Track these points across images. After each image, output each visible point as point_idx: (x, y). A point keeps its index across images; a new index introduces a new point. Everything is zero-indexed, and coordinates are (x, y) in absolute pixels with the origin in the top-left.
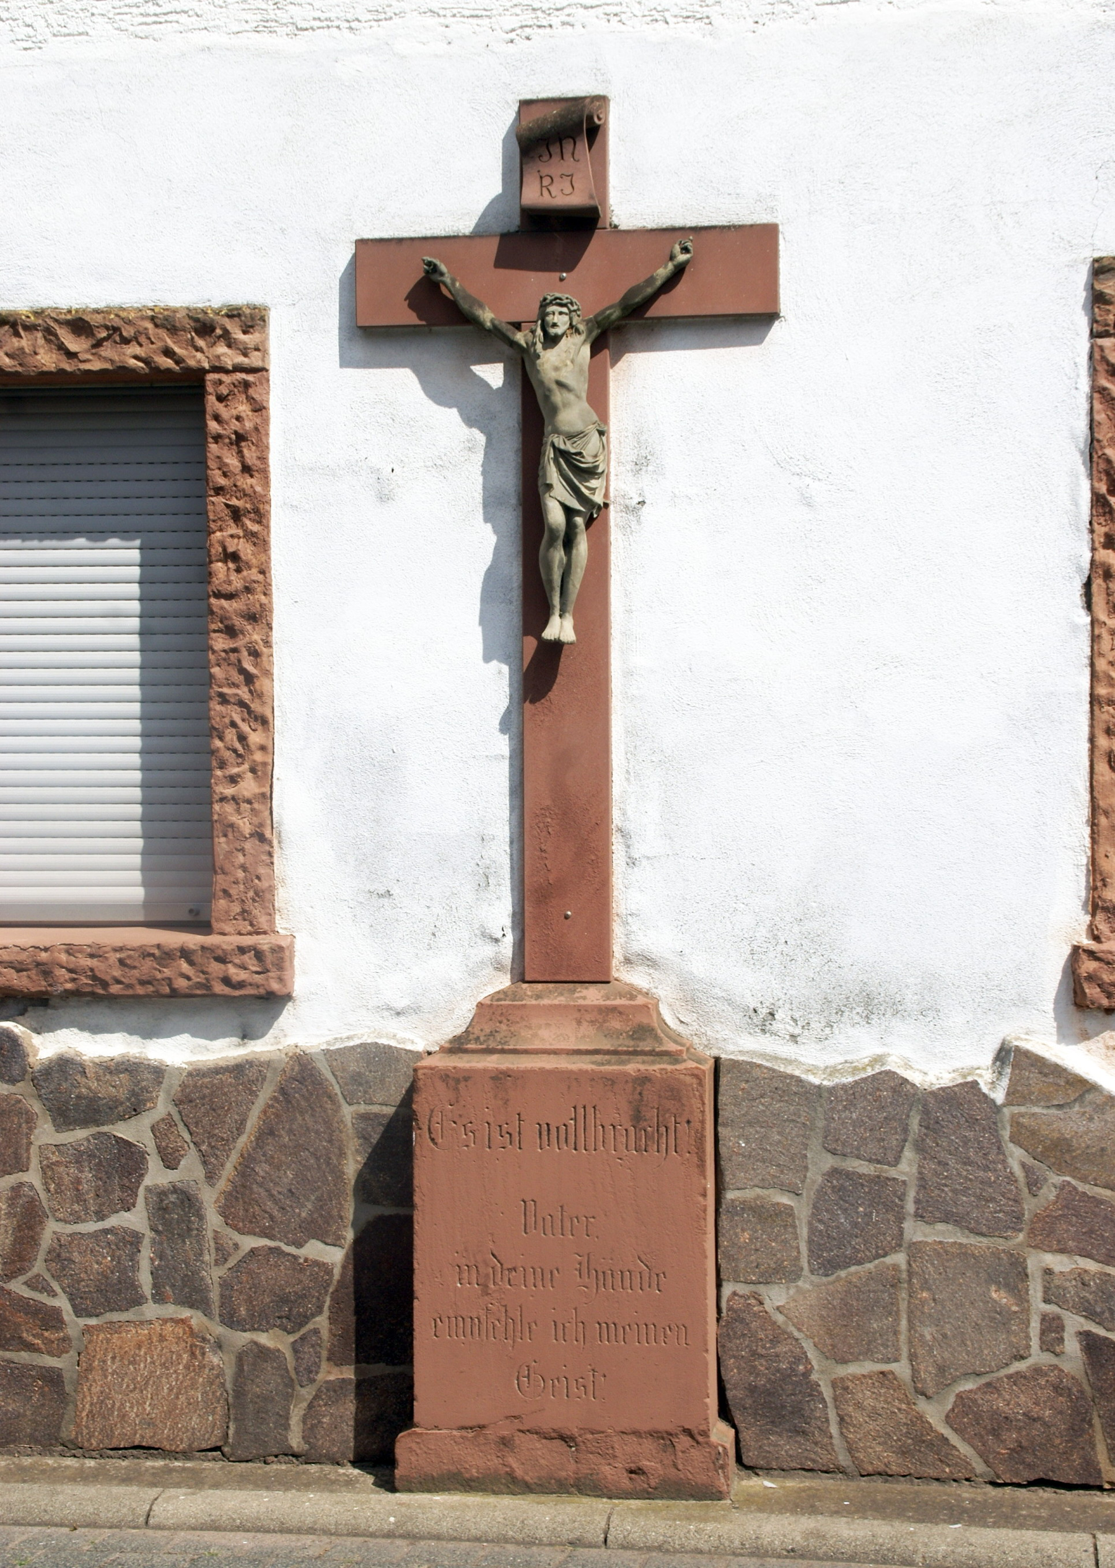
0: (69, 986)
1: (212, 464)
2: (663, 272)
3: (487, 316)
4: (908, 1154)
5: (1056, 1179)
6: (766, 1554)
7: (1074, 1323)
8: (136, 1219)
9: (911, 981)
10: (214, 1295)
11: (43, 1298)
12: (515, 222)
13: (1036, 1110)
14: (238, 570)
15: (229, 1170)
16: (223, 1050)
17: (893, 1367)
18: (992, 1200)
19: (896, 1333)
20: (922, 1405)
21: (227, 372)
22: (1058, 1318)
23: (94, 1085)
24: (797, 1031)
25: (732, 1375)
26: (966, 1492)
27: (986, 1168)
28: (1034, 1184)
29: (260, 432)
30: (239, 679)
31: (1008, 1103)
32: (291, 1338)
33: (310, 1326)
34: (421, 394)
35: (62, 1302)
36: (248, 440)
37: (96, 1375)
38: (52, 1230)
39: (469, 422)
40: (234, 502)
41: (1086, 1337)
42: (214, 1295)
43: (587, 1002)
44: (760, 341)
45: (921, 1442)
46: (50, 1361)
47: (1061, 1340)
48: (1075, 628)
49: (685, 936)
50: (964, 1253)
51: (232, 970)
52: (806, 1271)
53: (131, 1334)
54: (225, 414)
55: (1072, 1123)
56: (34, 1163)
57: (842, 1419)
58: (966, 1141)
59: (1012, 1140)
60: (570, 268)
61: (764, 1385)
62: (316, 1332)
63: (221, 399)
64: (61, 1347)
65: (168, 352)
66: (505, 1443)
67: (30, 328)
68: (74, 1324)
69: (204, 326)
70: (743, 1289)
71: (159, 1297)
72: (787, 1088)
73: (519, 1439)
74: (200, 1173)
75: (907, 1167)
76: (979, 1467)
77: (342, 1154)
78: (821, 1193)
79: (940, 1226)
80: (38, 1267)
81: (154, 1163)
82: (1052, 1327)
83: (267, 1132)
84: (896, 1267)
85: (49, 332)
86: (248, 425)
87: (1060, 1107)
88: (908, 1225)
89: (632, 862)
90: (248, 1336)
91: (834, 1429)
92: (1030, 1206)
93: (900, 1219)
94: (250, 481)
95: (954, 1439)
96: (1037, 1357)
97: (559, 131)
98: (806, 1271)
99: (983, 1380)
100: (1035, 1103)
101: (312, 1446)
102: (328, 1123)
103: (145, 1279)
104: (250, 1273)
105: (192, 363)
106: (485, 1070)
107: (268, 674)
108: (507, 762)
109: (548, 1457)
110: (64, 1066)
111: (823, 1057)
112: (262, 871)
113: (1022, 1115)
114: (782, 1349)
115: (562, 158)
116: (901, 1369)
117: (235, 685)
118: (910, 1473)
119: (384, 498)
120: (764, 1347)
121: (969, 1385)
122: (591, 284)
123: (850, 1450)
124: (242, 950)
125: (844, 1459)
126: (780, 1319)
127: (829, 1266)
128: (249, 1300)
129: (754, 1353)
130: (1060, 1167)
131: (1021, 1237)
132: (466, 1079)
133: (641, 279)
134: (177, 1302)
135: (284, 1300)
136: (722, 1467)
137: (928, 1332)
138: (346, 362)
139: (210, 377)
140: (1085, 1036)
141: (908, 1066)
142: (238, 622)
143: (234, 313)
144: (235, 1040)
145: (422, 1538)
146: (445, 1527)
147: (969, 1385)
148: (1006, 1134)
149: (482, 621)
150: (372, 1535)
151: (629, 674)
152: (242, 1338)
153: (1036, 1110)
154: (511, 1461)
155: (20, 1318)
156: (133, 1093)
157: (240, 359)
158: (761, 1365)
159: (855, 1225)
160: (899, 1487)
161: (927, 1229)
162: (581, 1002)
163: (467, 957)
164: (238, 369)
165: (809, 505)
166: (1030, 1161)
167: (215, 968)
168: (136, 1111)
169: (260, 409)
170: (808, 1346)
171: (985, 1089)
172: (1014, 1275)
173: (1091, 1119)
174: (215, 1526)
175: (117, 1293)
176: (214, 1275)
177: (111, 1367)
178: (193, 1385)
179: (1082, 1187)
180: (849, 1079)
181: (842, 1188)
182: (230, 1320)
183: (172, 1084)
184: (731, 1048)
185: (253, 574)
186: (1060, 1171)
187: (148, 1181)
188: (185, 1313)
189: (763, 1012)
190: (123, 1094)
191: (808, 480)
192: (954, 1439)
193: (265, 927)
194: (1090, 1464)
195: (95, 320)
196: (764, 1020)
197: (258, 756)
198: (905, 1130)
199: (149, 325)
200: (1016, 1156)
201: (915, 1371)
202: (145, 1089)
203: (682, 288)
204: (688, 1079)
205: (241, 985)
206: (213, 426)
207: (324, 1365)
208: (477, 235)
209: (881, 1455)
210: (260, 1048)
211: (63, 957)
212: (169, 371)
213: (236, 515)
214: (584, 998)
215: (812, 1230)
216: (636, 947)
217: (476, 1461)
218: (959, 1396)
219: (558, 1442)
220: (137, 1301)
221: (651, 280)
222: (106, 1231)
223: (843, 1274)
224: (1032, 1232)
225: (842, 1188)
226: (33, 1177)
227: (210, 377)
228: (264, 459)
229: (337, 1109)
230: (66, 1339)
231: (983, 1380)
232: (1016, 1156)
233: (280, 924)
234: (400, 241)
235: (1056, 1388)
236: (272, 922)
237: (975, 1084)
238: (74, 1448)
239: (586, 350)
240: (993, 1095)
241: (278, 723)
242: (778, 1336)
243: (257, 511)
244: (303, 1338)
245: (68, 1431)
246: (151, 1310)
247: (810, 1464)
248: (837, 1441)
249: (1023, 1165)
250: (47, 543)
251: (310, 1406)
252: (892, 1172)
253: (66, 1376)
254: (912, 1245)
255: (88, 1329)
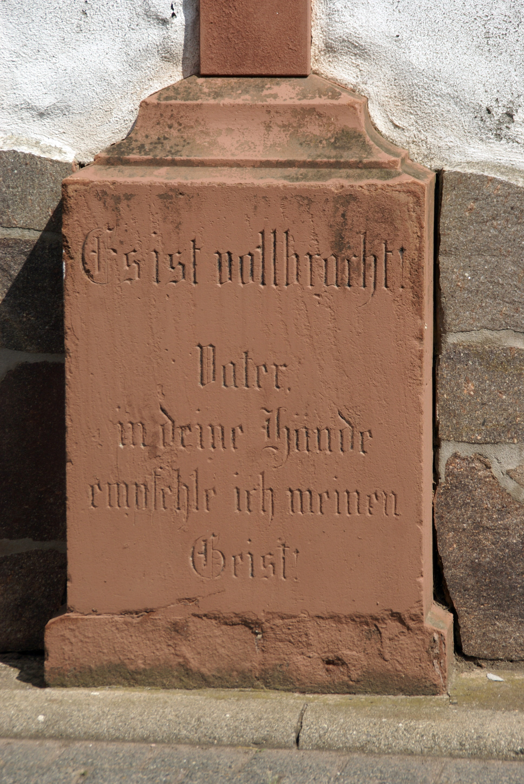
6: (490, 756)
25: (451, 552)
43: (279, 102)
61: (490, 563)
66: (177, 629)
70: (465, 450)
106: (151, 186)
114: (511, 520)
120: (490, 518)
126: (510, 485)
129: (478, 526)
132: (128, 197)
136: (438, 657)
145: (78, 738)
146: (105, 726)
150: (17, 736)
154: (185, 650)
158: (486, 540)
162: (271, 101)
163: (127, 43)
184: (457, 158)
189: (499, 111)
204: (403, 198)
214: (275, 96)
216: (340, 31)
217: (141, 650)
219: (241, 629)
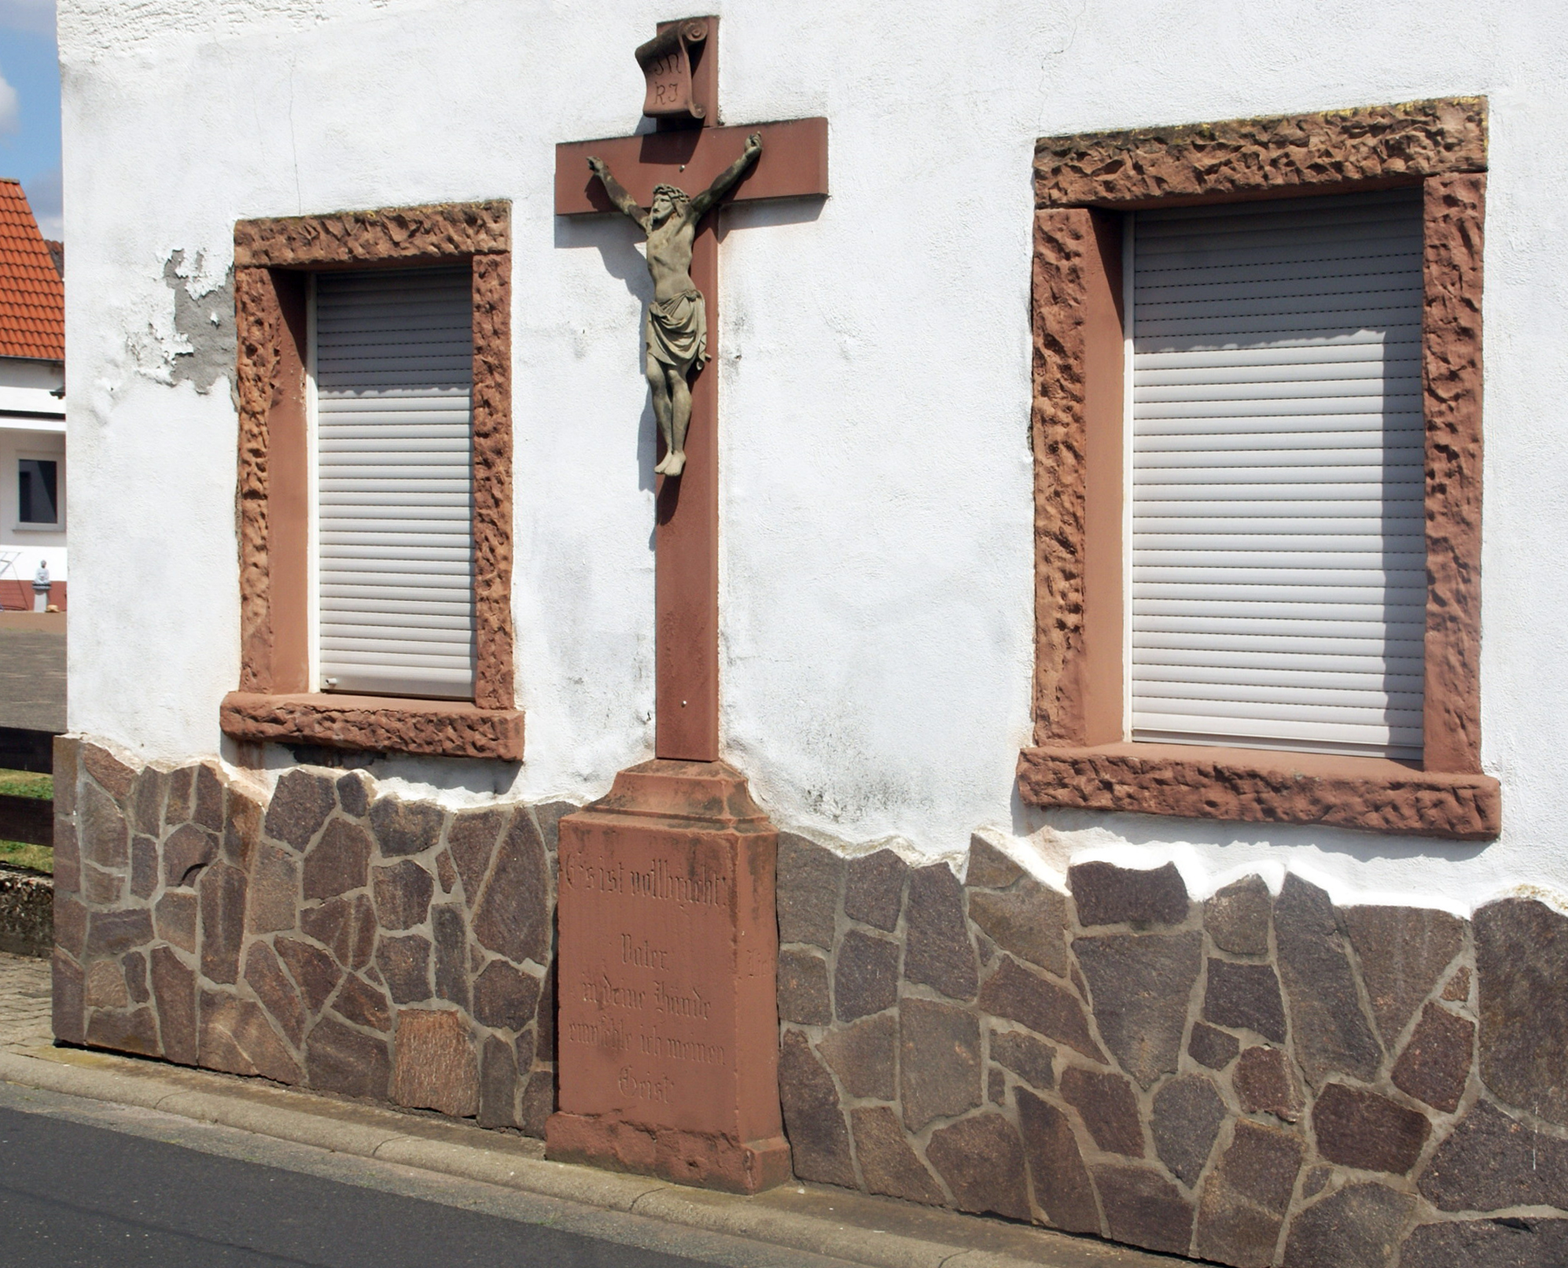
0: (386, 743)
1: (475, 329)
2: (739, 162)
3: (627, 203)
4: (901, 922)
5: (1001, 952)
6: (727, 1232)
7: (1012, 1079)
8: (425, 930)
9: (914, 773)
10: (471, 995)
11: (374, 985)
12: (652, 125)
13: (987, 891)
14: (491, 414)
15: (479, 897)
16: (481, 801)
17: (891, 1104)
18: (956, 967)
19: (893, 1075)
20: (911, 1139)
21: (485, 254)
22: (1000, 1073)
23: (403, 822)
24: (838, 812)
25: (788, 1098)
26: (932, 1215)
27: (953, 939)
28: (985, 955)
29: (505, 300)
30: (491, 502)
31: (968, 884)
32: (516, 1036)
33: (526, 1028)
34: (603, 268)
35: (385, 990)
36: (498, 307)
37: (405, 1049)
38: (380, 932)
39: (632, 290)
40: (490, 359)
41: (1019, 1091)
42: (471, 995)
44: (815, 217)
45: (908, 1171)
46: (380, 1035)
47: (1002, 1093)
48: (1023, 466)
49: (756, 722)
50: (936, 1011)
51: (477, 736)
52: (834, 1017)
53: (426, 1020)
54: (485, 287)
55: (1010, 904)
56: (370, 882)
57: (858, 1147)
58: (940, 914)
59: (971, 916)
60: (686, 162)
62: (530, 1032)
63: (482, 276)
64: (385, 1025)
65: (450, 240)
66: (612, 1130)
67: (373, 224)
68: (395, 1008)
69: (471, 217)
70: (795, 1028)
71: (440, 995)
72: (817, 858)
73: (622, 1128)
74: (463, 898)
75: (899, 934)
76: (949, 1197)
77: (545, 892)
78: (843, 949)
79: (922, 987)
80: (372, 961)
81: (437, 886)
82: (996, 1080)
83: (501, 870)
84: (892, 1018)
85: (384, 226)
86: (496, 296)
87: (1002, 889)
88: (900, 983)
89: (731, 662)
90: (490, 1030)
91: (852, 1153)
92: (982, 975)
93: (895, 978)
94: (498, 342)
95: (931, 1170)
96: (988, 1107)
98: (834, 1017)
99: (951, 1122)
100: (986, 885)
101: (528, 1123)
102: (537, 865)
103: (432, 978)
104: (491, 980)
105: (464, 248)
106: (600, 826)
107: (509, 498)
108: (653, 575)
109: (632, 1144)
110: (387, 805)
111: (852, 836)
112: (505, 658)
113: (977, 894)
114: (819, 1081)
116: (895, 1106)
117: (489, 507)
118: (898, 1195)
119: (579, 355)
121: (941, 1126)
122: (694, 177)
123: (864, 1172)
124: (484, 721)
125: (859, 1180)
126: (817, 1055)
127: (849, 1013)
128: (491, 1002)
129: (801, 1083)
130: (1003, 943)
131: (976, 1000)
132: (589, 832)
133: (722, 171)
134: (451, 999)
135: (511, 1004)
136: (750, 1169)
137: (913, 1077)
138: (560, 243)
139: (476, 258)
140: (1030, 829)
141: (910, 847)
142: (491, 456)
143: (488, 207)
144: (490, 794)
145: (524, 1189)
146: (540, 1184)
147: (941, 1126)
148: (967, 910)
149: (639, 456)
150: (496, 1183)
151: (730, 502)
152: (487, 1031)
153: (987, 891)
154: (616, 1145)
155: (363, 999)
156: (425, 831)
157: (493, 244)
158: (806, 1092)
159: (865, 980)
160: (890, 1205)
161: (913, 988)
163: (628, 735)
164: (492, 251)
165: (846, 358)
166: (983, 935)
167: (468, 733)
168: (426, 845)
169: (505, 283)
170: (835, 1079)
171: (953, 871)
172: (969, 1032)
173: (1023, 902)
174: (409, 1163)
175: (412, 988)
176: (471, 979)
177: (414, 1044)
178: (459, 1066)
179: (1018, 961)
180: (862, 855)
181: (857, 948)
182: (480, 1017)
183: (448, 824)
184: (794, 823)
185: (498, 417)
186: (1003, 946)
187: (433, 902)
188: (454, 1007)
189: (815, 793)
190: (418, 830)
191: (846, 337)
192: (931, 1170)
193: (506, 704)
194: (1022, 1202)
195: (408, 216)
196: (815, 801)
197: (503, 565)
198: (899, 902)
199: (440, 219)
200: (973, 928)
201: (905, 1110)
202: (432, 828)
203: (758, 175)
204: (724, 843)
205: (481, 749)
206: (477, 297)
207: (535, 1059)
208: (636, 135)
209: (883, 1179)
210: (505, 801)
211: (384, 720)
212: (451, 254)
213: (491, 369)
215: (838, 982)
216: (733, 733)
217: (595, 1142)
218: (935, 1134)
219: (645, 1135)
220: (426, 995)
221: (731, 169)
222: (410, 938)
223: (858, 1021)
224: (982, 998)
225: (857, 948)
226: (368, 891)
227: (476, 258)
228: (506, 323)
229: (542, 854)
230: (388, 1019)
231: (951, 1122)
232: (973, 928)
233: (518, 702)
234: (581, 143)
235: (1001, 1134)
236: (511, 699)
237: (946, 864)
238: (394, 1104)
239: (689, 231)
240: (958, 876)
241: (515, 539)
242: (817, 1070)
243: (501, 366)
244: (522, 1036)
245: (391, 1092)
246: (435, 1003)
247: (837, 1180)
248: (854, 1162)
249: (978, 938)
250: (390, 392)
251: (527, 1092)
252: (890, 937)
253: (390, 1048)
254: (903, 1000)
255: (400, 1013)
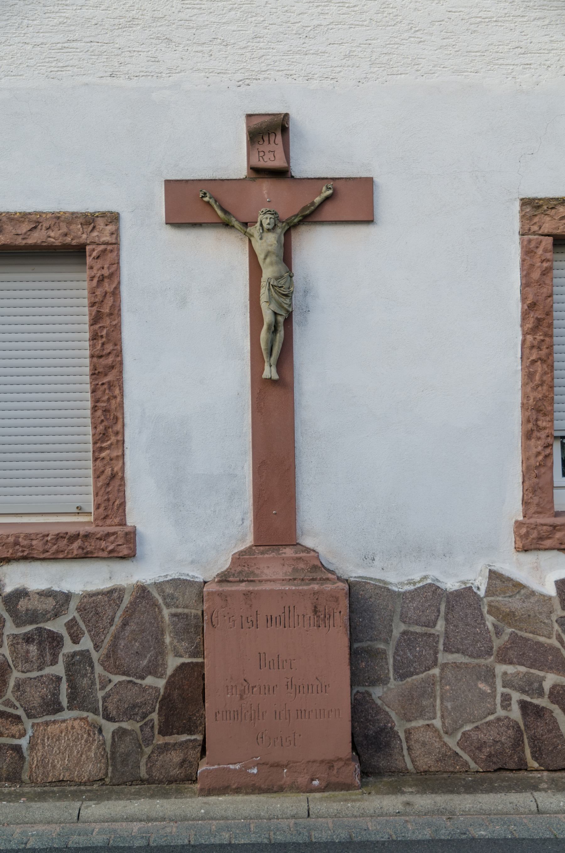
7: (516, 696)
17: (434, 722)
19: (434, 706)
28: (498, 632)
31: (486, 596)
43: (287, 555)
47: (510, 704)
55: (515, 604)
61: (372, 734)
62: (152, 720)
71: (70, 708)
84: (434, 676)
87: (510, 597)
92: (497, 643)
93: (436, 653)
97: (269, 130)
113: (492, 601)
115: (269, 143)
120: (372, 716)
121: (468, 727)
126: (379, 702)
129: (367, 720)
137: (449, 705)
152: (116, 725)
162: (284, 555)
172: (489, 675)
179: (520, 633)
180: (412, 587)
186: (510, 625)
188: (85, 714)
198: (439, 611)
201: (443, 723)
214: (285, 553)
218: (464, 734)
220: (60, 709)
232: (490, 620)
237: (470, 588)
244: (146, 724)
249: (493, 625)
251: (149, 757)
252: (432, 631)
